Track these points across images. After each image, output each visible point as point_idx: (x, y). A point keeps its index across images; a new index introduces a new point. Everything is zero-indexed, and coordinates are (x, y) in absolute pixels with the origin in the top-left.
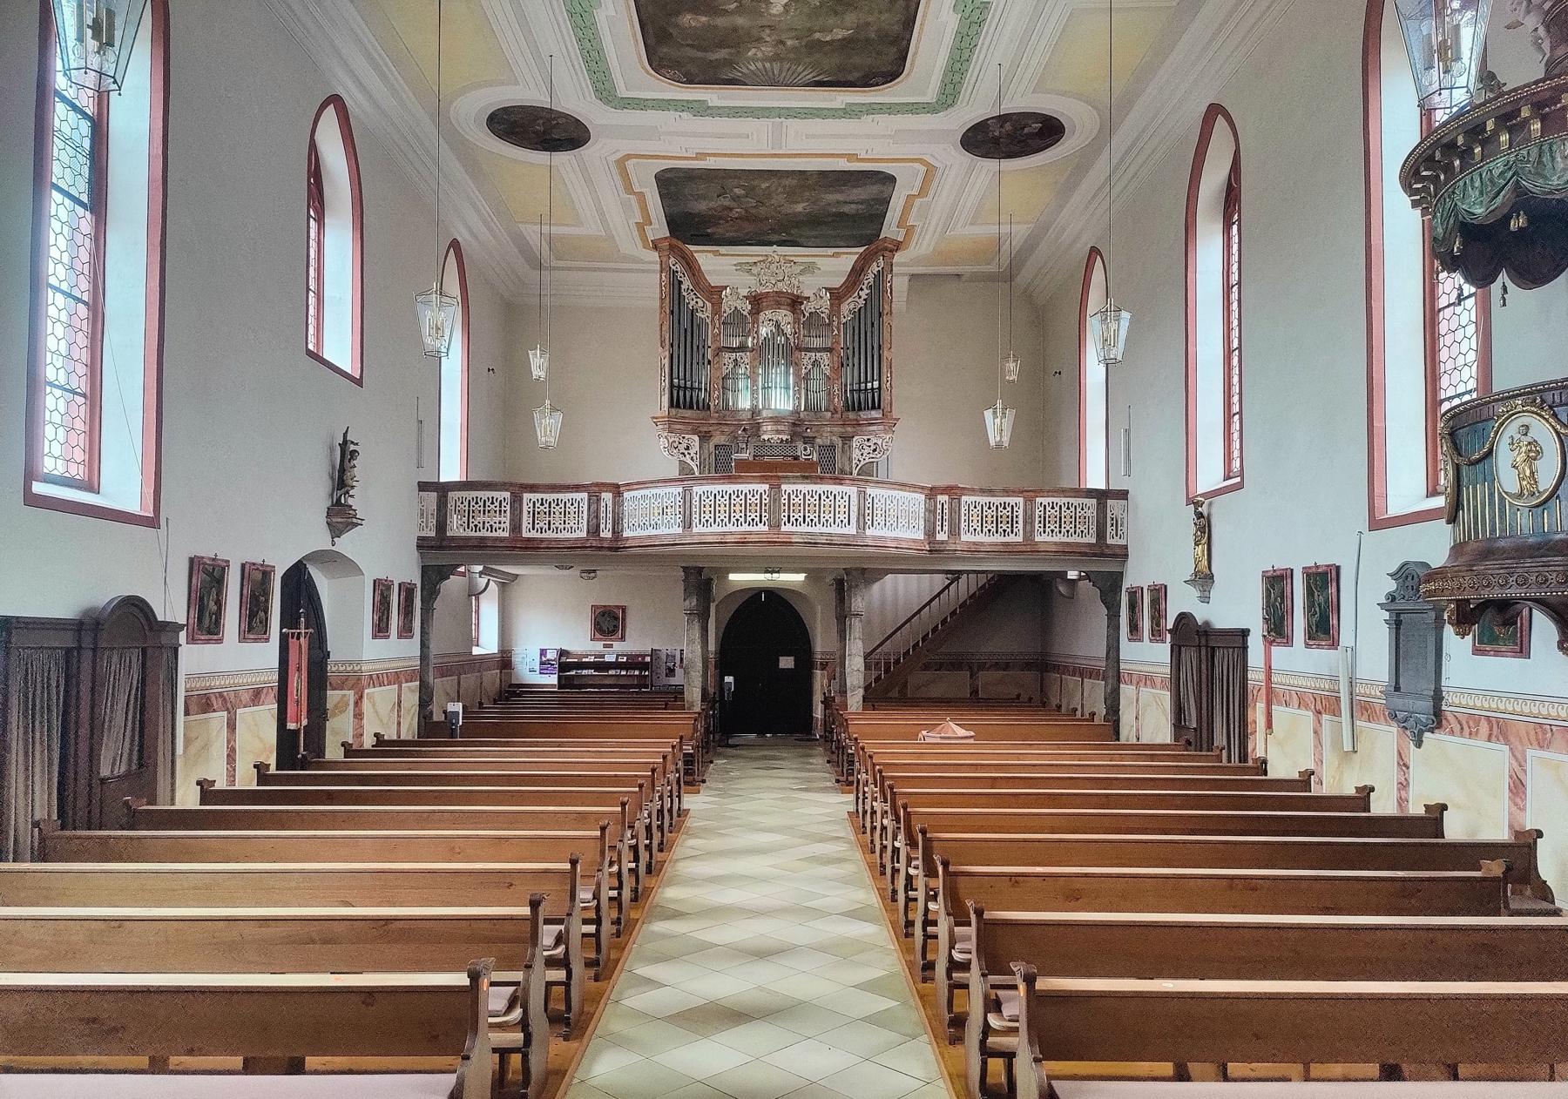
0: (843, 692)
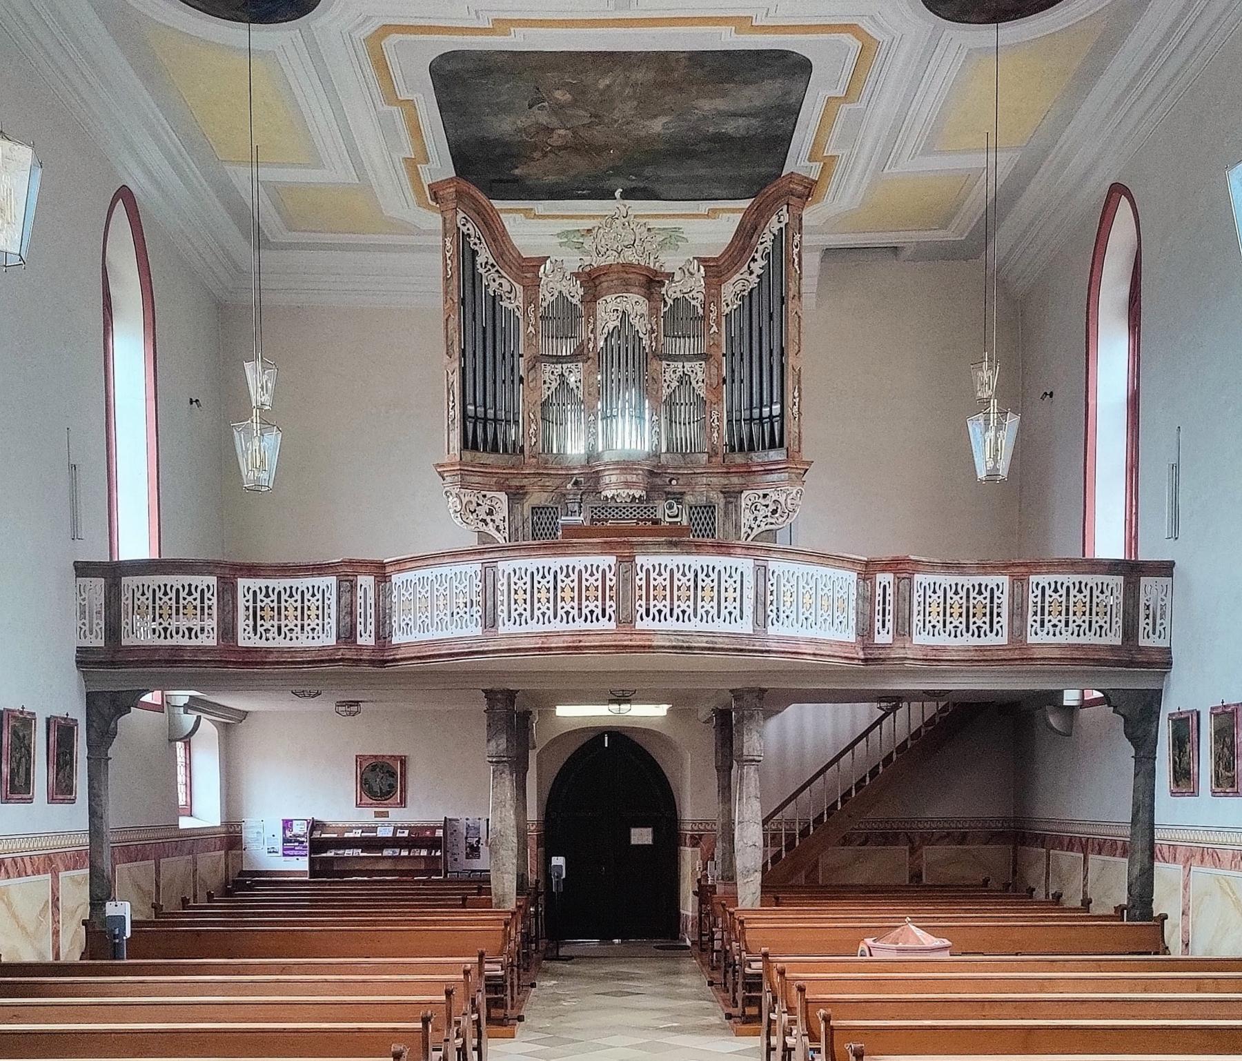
0: (729, 877)
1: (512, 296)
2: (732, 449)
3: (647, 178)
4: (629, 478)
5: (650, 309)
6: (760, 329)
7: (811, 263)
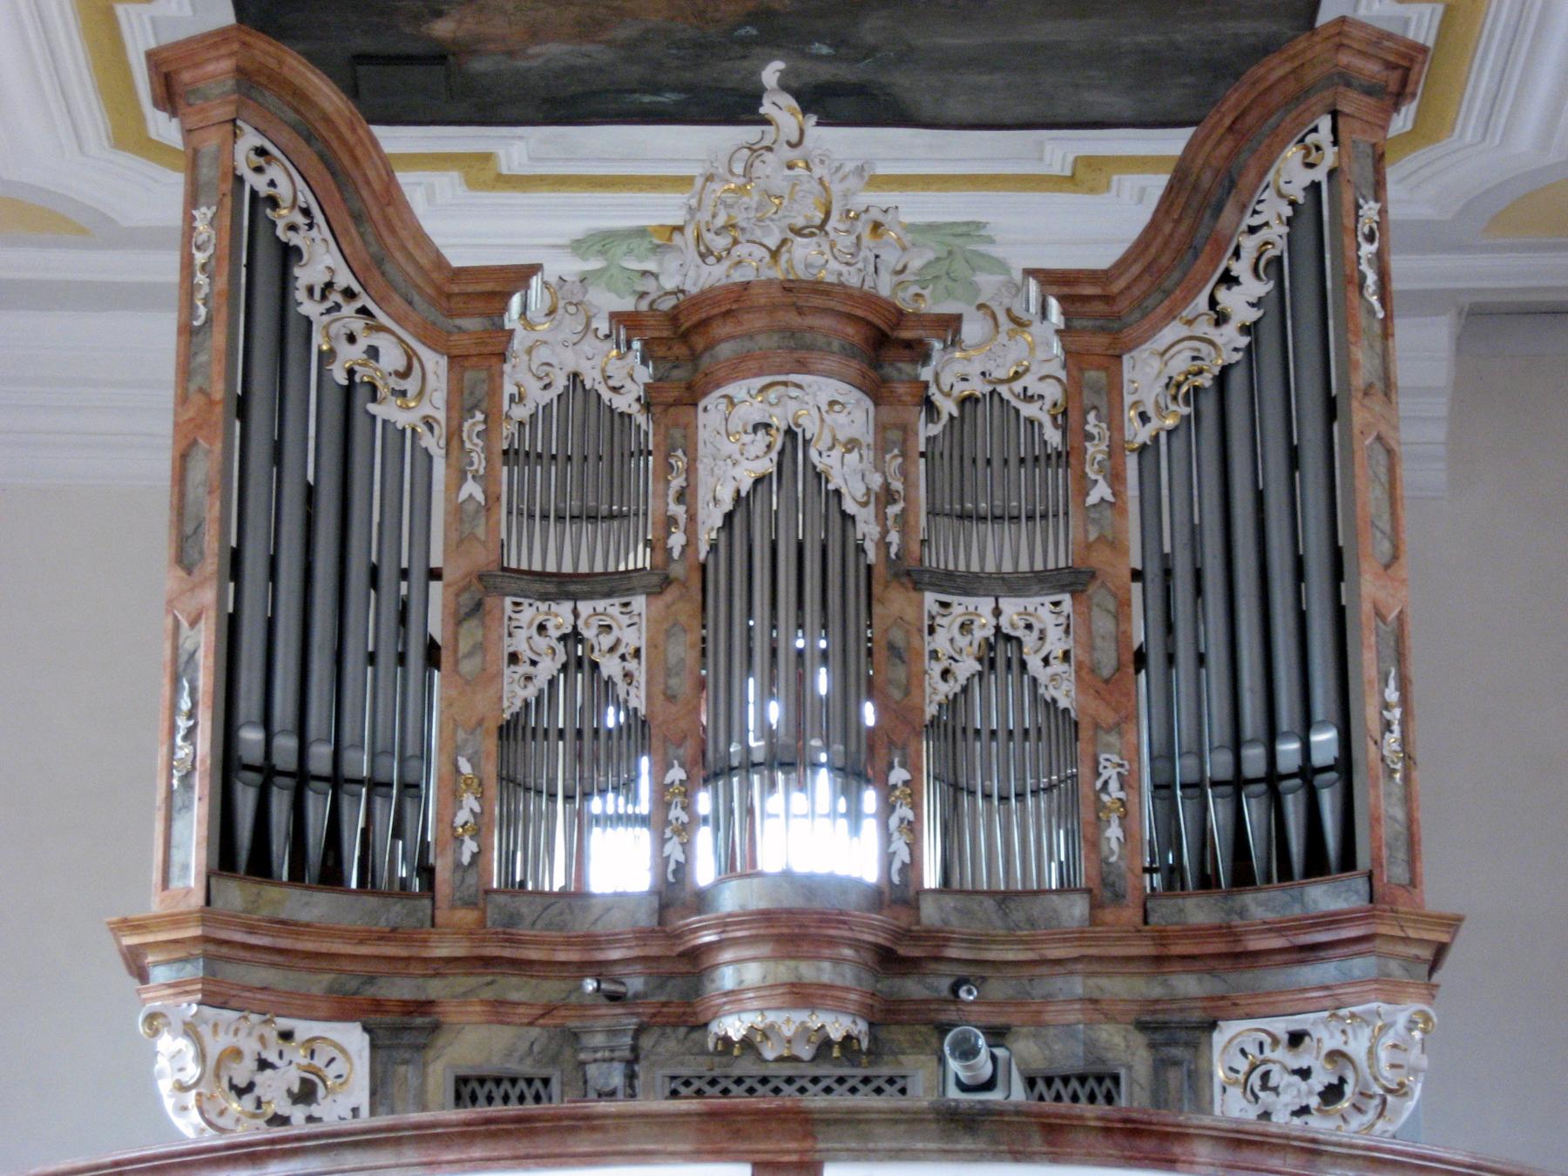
1: (411, 385)
2: (1173, 876)
3: (871, 51)
4: (809, 971)
5: (881, 428)
6: (1260, 498)
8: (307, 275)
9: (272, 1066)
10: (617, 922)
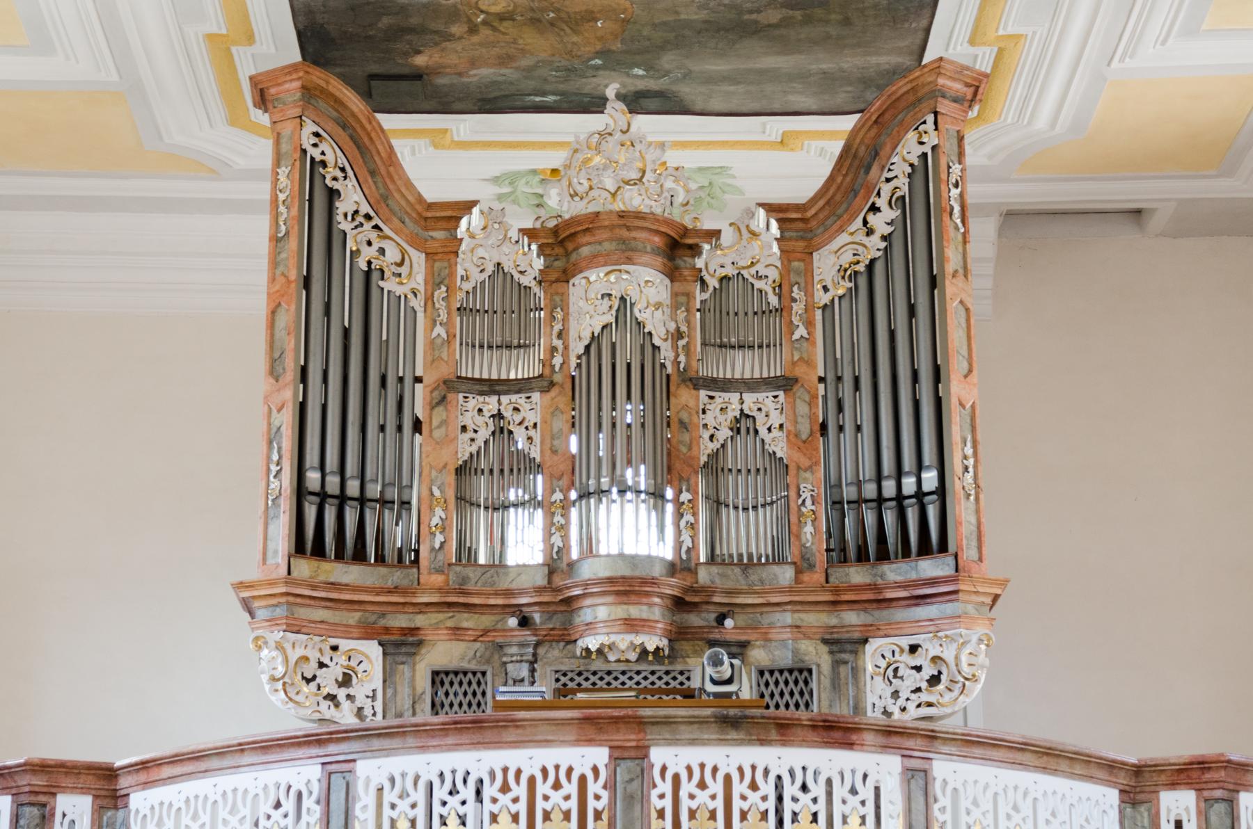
1: (404, 270)
3: (667, 73)
4: (635, 611)
5: (675, 295)
6: (892, 335)
7: (984, 231)
8: (342, 207)
9: (327, 666)
10: (525, 582)
